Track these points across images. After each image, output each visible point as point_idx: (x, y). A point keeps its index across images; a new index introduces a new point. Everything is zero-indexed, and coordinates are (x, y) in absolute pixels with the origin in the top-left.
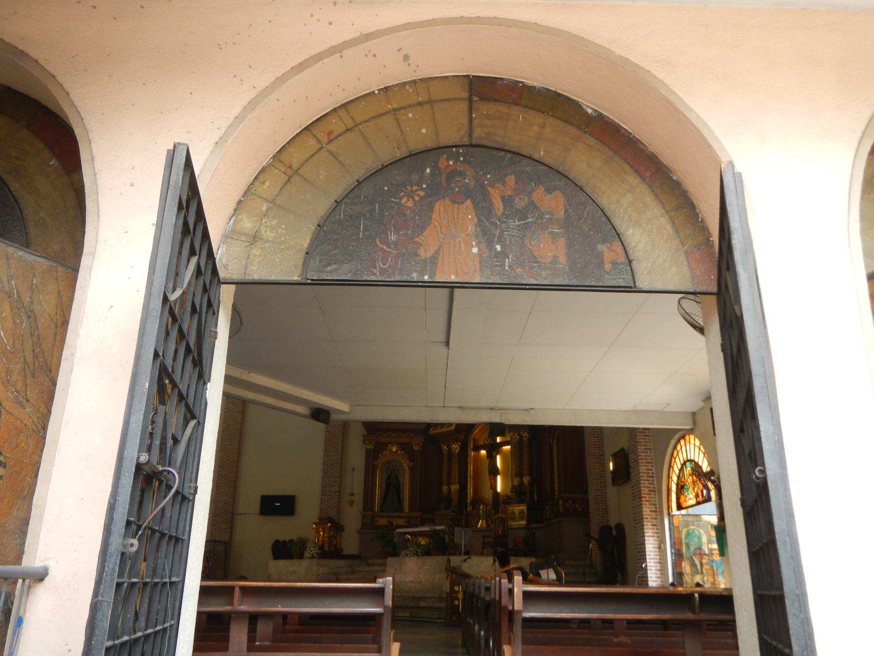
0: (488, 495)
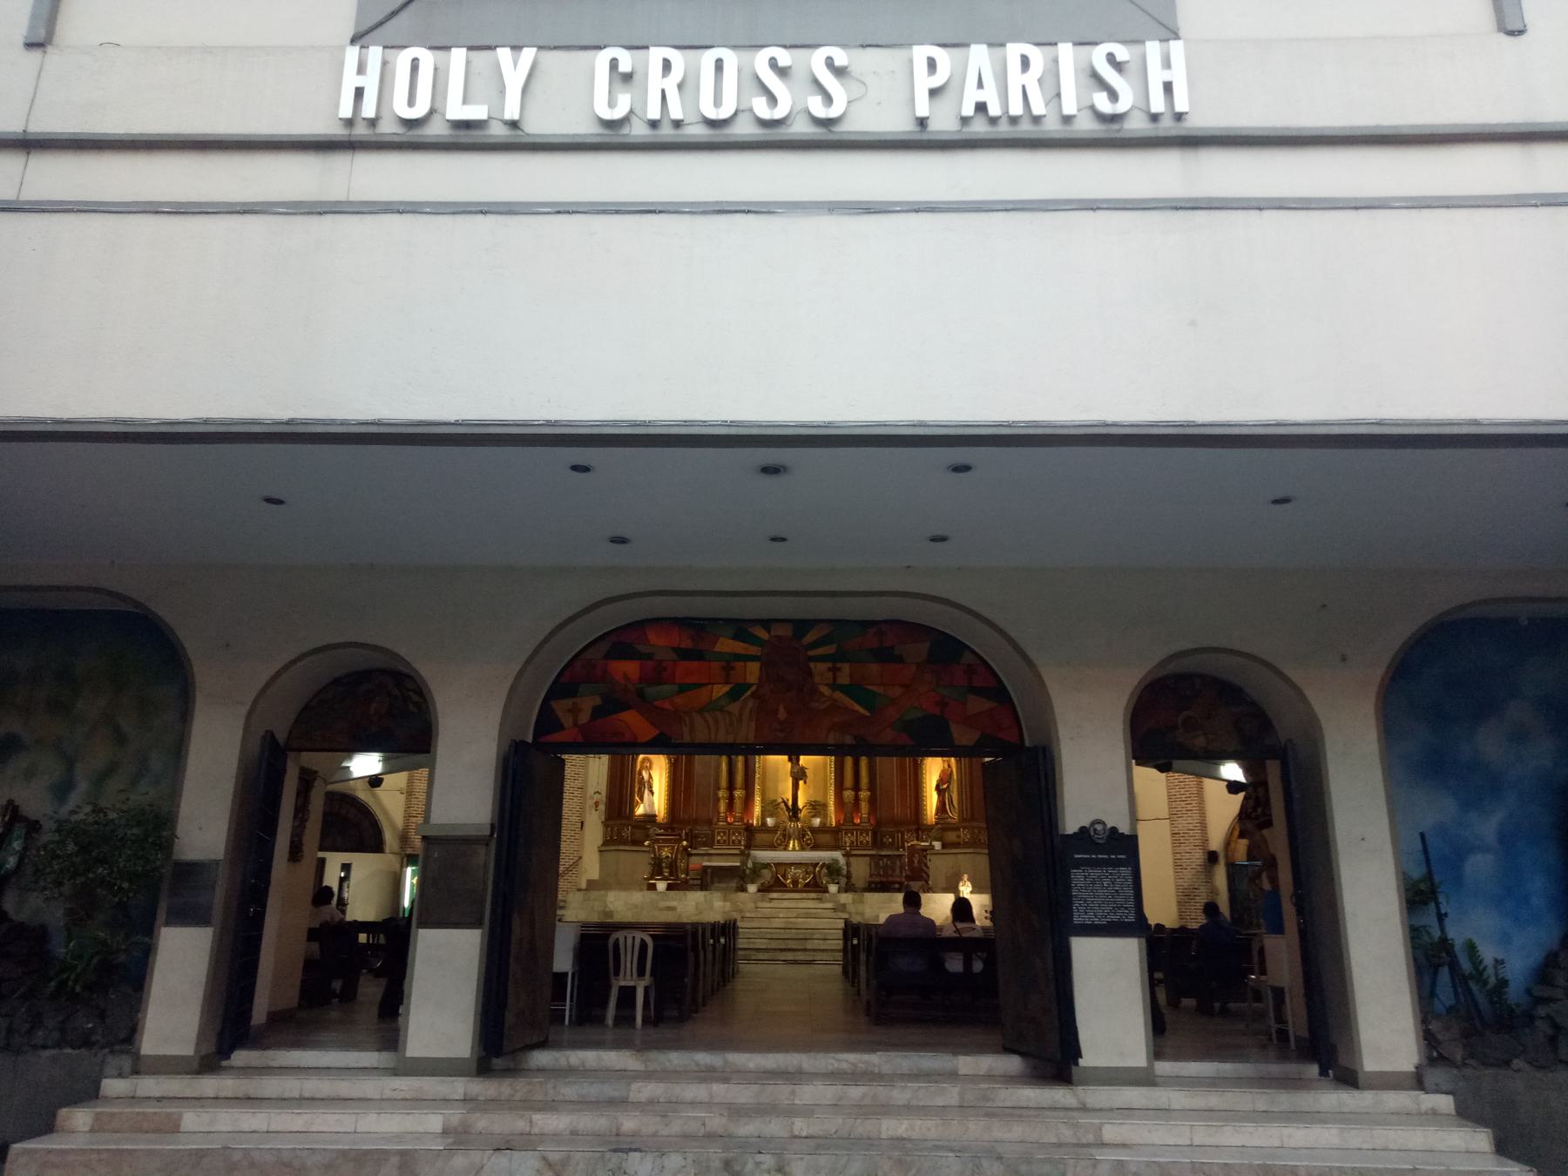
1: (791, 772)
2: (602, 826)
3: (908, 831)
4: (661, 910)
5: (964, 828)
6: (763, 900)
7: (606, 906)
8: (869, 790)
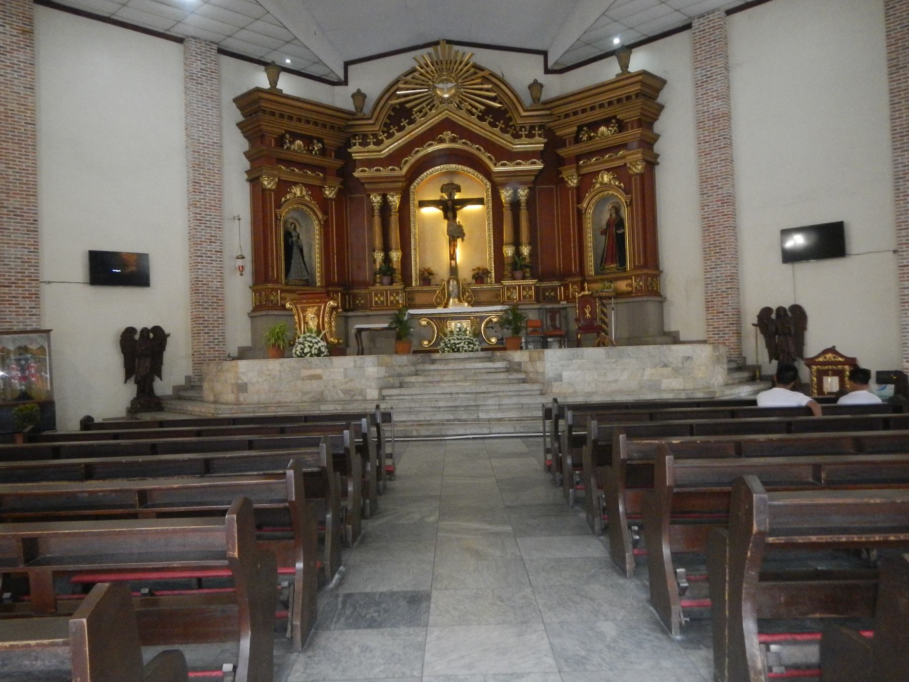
0: (441, 268)
2: (250, 291)
3: (573, 283)
4: (303, 379)
6: (424, 362)
7: (238, 378)
8: (530, 244)
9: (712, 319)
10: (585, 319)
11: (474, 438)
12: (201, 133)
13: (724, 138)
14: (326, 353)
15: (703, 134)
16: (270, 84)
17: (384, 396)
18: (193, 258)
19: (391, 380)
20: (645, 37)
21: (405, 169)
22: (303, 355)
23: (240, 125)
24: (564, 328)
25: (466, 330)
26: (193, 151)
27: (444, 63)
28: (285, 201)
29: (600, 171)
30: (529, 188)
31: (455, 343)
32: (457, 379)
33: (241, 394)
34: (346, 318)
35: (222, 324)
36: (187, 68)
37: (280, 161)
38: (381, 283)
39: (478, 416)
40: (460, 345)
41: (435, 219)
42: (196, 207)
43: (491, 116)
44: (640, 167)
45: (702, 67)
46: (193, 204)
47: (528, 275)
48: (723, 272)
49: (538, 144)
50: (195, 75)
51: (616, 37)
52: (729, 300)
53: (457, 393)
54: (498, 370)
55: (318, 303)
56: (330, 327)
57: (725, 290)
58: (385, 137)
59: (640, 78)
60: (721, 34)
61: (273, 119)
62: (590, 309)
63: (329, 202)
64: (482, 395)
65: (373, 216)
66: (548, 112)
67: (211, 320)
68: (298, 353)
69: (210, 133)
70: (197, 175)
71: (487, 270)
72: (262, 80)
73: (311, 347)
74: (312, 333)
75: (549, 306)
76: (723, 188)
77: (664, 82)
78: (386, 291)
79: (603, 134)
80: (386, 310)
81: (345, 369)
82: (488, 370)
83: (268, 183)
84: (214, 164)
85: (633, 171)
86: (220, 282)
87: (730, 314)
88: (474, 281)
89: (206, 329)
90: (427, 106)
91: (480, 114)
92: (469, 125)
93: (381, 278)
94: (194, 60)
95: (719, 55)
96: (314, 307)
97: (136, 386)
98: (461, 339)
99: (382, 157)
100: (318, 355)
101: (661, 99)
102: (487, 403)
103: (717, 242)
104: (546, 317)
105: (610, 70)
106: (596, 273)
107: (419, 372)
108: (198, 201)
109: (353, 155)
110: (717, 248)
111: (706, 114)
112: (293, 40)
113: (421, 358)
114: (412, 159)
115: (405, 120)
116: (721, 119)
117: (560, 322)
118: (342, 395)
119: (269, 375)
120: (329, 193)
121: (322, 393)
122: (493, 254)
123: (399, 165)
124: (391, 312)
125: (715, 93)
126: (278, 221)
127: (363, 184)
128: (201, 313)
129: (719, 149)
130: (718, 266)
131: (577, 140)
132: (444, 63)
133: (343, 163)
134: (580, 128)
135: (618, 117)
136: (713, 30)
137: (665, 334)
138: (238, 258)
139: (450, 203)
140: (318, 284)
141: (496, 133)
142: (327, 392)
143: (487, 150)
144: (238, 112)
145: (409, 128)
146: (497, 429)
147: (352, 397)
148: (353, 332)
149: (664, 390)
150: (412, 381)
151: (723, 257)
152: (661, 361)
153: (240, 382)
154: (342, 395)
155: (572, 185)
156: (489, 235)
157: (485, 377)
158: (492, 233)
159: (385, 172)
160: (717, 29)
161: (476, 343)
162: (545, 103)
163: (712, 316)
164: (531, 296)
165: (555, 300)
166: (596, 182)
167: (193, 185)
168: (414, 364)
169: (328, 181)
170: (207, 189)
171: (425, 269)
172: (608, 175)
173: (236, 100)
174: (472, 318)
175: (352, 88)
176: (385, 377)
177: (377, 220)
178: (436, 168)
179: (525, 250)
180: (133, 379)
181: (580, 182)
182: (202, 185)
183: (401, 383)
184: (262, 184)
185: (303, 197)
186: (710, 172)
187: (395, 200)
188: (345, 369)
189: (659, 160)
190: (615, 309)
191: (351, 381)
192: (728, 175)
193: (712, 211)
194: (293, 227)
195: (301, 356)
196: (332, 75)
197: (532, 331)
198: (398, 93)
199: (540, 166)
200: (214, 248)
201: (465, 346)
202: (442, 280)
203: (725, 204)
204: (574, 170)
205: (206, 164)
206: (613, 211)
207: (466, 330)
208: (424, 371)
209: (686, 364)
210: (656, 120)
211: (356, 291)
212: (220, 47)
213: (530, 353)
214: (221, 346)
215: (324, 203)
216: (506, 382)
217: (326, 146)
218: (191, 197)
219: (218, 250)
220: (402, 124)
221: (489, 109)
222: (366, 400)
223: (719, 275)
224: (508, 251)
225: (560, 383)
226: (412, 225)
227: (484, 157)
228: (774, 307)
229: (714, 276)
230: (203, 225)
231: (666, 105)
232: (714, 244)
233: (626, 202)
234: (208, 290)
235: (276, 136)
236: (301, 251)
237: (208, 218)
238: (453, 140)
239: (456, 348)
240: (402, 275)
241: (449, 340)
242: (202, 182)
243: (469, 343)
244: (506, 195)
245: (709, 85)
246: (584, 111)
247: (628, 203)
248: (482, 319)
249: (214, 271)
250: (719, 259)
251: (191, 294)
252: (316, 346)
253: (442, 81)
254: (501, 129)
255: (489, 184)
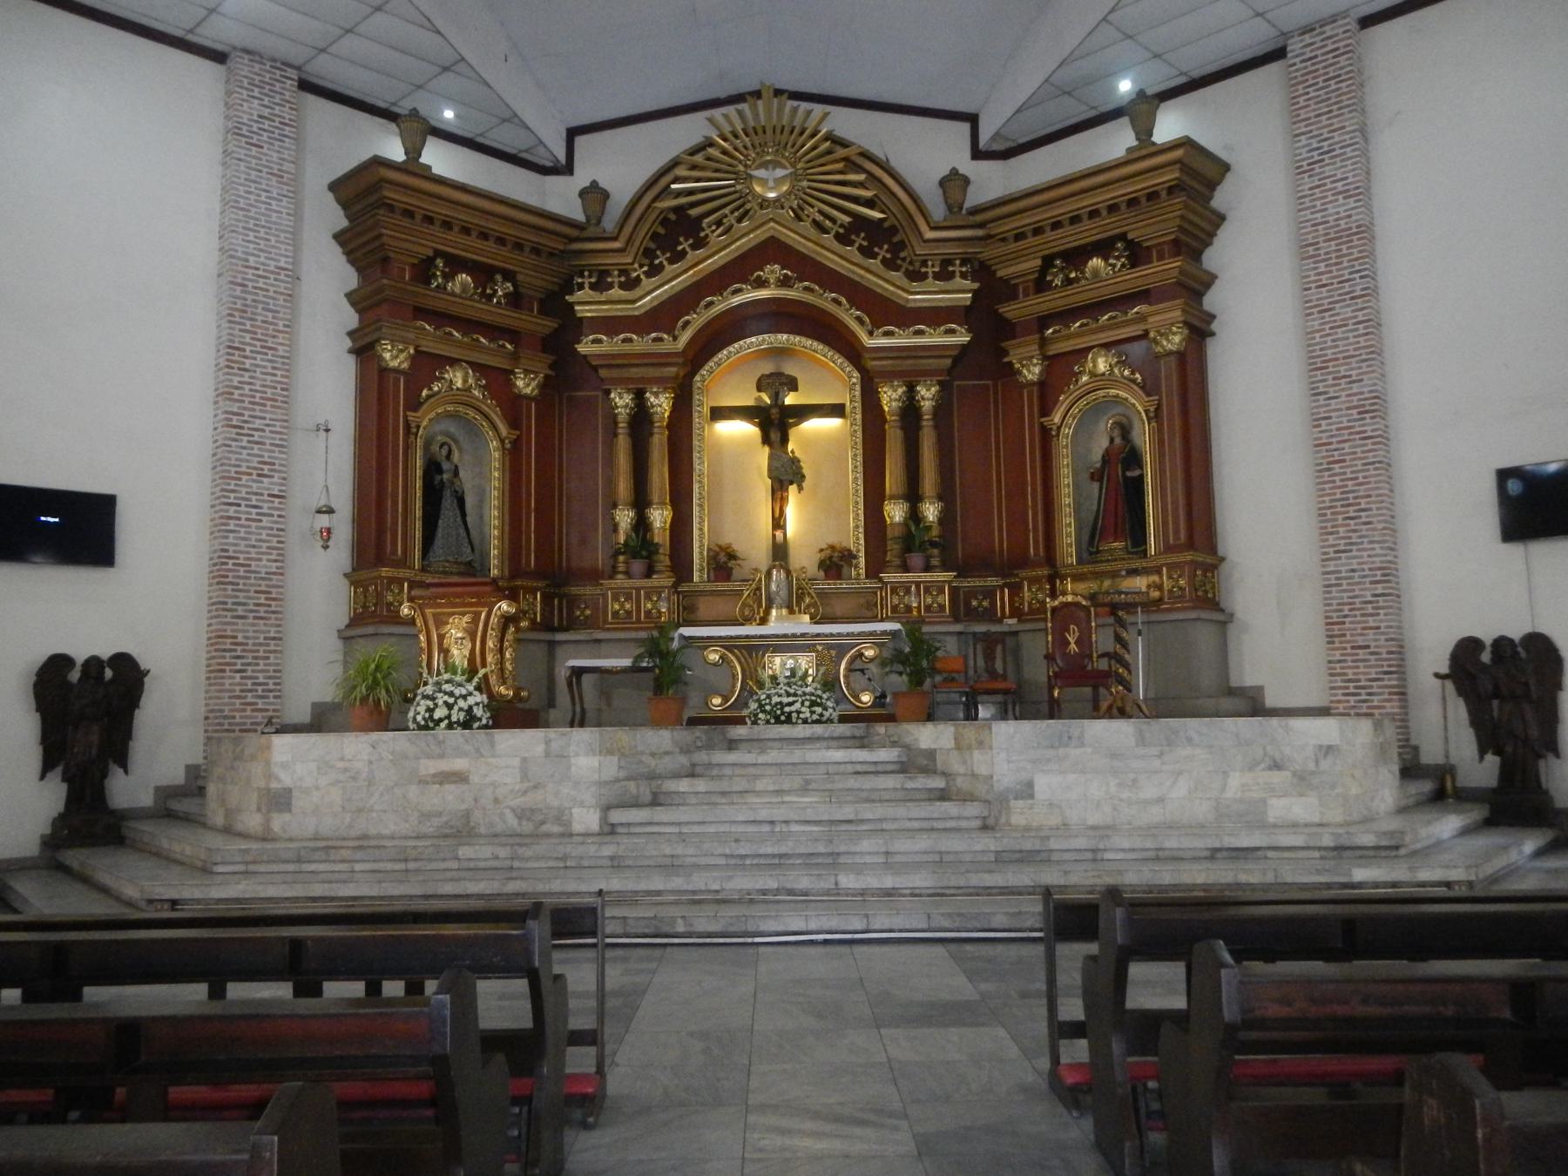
0: (754, 543)
1: (770, 470)
2: (346, 582)
3: (1032, 581)
4: (423, 782)
5: (1171, 567)
6: (710, 746)
8: (940, 498)
9: (1339, 661)
10: (1066, 656)
11: (826, 942)
12: (252, 246)
13: (1361, 277)
14: (484, 721)
15: (1315, 268)
16: (406, 153)
17: (613, 825)
18: (218, 508)
19: (632, 785)
20: (1182, 80)
21: (685, 337)
22: (430, 724)
23: (340, 238)
24: (1011, 675)
25: (806, 674)
26: (232, 283)
27: (770, 132)
28: (429, 397)
29: (1091, 348)
30: (940, 383)
31: (781, 703)
32: (786, 786)
33: (275, 815)
34: (552, 645)
35: (275, 651)
36: (232, 113)
37: (421, 312)
38: (628, 574)
39: (836, 884)
40: (793, 708)
41: (744, 443)
42: (230, 400)
43: (863, 235)
44: (1177, 339)
45: (1311, 131)
46: (225, 394)
47: (935, 562)
48: (1365, 559)
49: (960, 293)
50: (245, 128)
51: (1125, 77)
52: (1381, 621)
53: (786, 822)
54: (880, 768)
55: (472, 605)
56: (501, 662)
57: (1370, 599)
58: (645, 273)
59: (1179, 153)
60: (1351, 65)
61: (406, 222)
62: (1077, 634)
63: (525, 402)
64: (844, 827)
65: (616, 435)
66: (980, 233)
67: (250, 642)
68: (419, 718)
69: (273, 247)
70: (237, 332)
71: (849, 550)
72: (395, 150)
73: (450, 707)
74: (455, 673)
75: (980, 628)
76: (1362, 380)
77: (1225, 168)
78: (638, 590)
79: (1096, 273)
80: (637, 629)
81: (524, 760)
82: (859, 768)
83: (393, 356)
84: (278, 312)
85: (1163, 346)
86: (276, 561)
87: (1384, 650)
88: (822, 574)
89: (239, 661)
90: (732, 212)
91: (841, 231)
92: (818, 253)
93: (626, 562)
94: (245, 97)
95: (1348, 106)
96: (463, 614)
97: (64, 787)
98: (795, 695)
99: (636, 313)
100: (466, 725)
101: (1219, 200)
102: (858, 849)
103: (1351, 495)
104: (975, 649)
105: (1117, 141)
106: (1080, 561)
107: (698, 770)
108: (237, 388)
109: (577, 308)
110: (1351, 508)
111: (1320, 227)
112: (456, 63)
113: (704, 738)
114: (698, 319)
115: (686, 240)
116: (1355, 237)
117: (1005, 662)
118: (512, 821)
119: (346, 770)
120: (525, 384)
121: (467, 815)
122: (862, 518)
123: (670, 330)
124: (643, 635)
125: (1339, 184)
126: (412, 437)
127: (595, 369)
128: (229, 628)
129: (1352, 298)
130: (1354, 548)
131: (1041, 285)
132: (770, 132)
133: (556, 325)
134: (1048, 261)
135: (1130, 236)
136: (1334, 57)
137: (1232, 692)
138: (319, 512)
139: (774, 411)
140: (494, 572)
141: (873, 268)
142: (477, 816)
143: (853, 303)
144: (339, 212)
145: (692, 256)
146: (884, 921)
147: (537, 828)
148: (562, 674)
149: (1275, 826)
150: (682, 790)
151: (1364, 527)
152: (1265, 755)
153: (274, 785)
154: (512, 821)
155: (1030, 377)
156: (856, 479)
157: (852, 783)
158: (860, 476)
159: (641, 344)
160: (1343, 54)
161: (830, 704)
162: (975, 211)
163: (1342, 655)
164: (942, 607)
165: (990, 615)
166: (1080, 372)
167: (228, 354)
168: (686, 750)
169: (523, 361)
170: (258, 362)
171: (720, 547)
172: (1106, 356)
173: (334, 187)
174: (820, 648)
175: (581, 178)
176: (617, 780)
177: (623, 443)
178: (748, 340)
179: (931, 512)
180: (59, 770)
181: (1047, 371)
182: (248, 353)
183: (655, 794)
184: (380, 358)
185: (468, 389)
186: (1331, 347)
187: (661, 403)
188: (524, 760)
189: (1214, 326)
190: (1144, 632)
191: (536, 787)
192: (1372, 353)
193: (1338, 429)
194: (444, 452)
195: (426, 728)
196: (541, 150)
197: (945, 680)
198: (673, 186)
199: (963, 338)
200: (268, 489)
201: (803, 709)
202: (756, 570)
203: (1367, 415)
204: (1036, 347)
205: (259, 311)
206: (1116, 433)
207: (806, 674)
208: (710, 765)
209: (1325, 764)
210: (1208, 244)
211: (574, 590)
212: (304, 76)
213: (956, 729)
214: (272, 700)
215: (513, 407)
216: (899, 795)
217: (522, 290)
218: (222, 378)
219: (276, 493)
220: (680, 248)
221: (860, 223)
222: (571, 835)
223: (1355, 567)
224: (895, 512)
225: (1030, 802)
226: (695, 455)
227: (849, 317)
228: (1488, 639)
229: (1343, 569)
230: (245, 438)
231: (1229, 218)
232: (1343, 499)
233: (1147, 412)
234: (249, 578)
235: (416, 261)
236: (461, 501)
237: (258, 423)
238: (784, 282)
239: (783, 713)
240: (671, 557)
241: (769, 697)
242: (248, 348)
243: (813, 704)
244: (890, 397)
245: (1327, 168)
246: (1056, 225)
247: (1152, 415)
248: (842, 650)
249: (264, 537)
250: (1355, 531)
251: (210, 585)
252: (461, 703)
253: (765, 165)
254: (885, 262)
255: (856, 374)
